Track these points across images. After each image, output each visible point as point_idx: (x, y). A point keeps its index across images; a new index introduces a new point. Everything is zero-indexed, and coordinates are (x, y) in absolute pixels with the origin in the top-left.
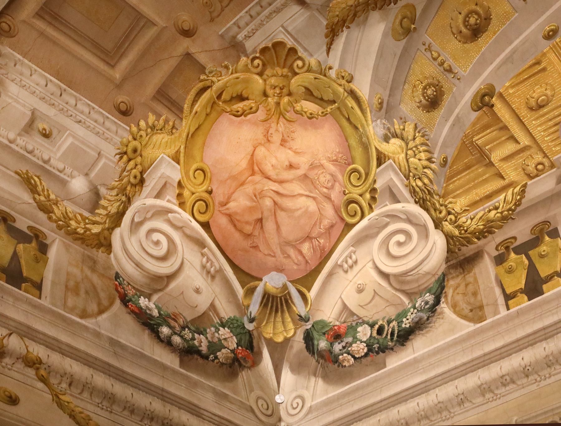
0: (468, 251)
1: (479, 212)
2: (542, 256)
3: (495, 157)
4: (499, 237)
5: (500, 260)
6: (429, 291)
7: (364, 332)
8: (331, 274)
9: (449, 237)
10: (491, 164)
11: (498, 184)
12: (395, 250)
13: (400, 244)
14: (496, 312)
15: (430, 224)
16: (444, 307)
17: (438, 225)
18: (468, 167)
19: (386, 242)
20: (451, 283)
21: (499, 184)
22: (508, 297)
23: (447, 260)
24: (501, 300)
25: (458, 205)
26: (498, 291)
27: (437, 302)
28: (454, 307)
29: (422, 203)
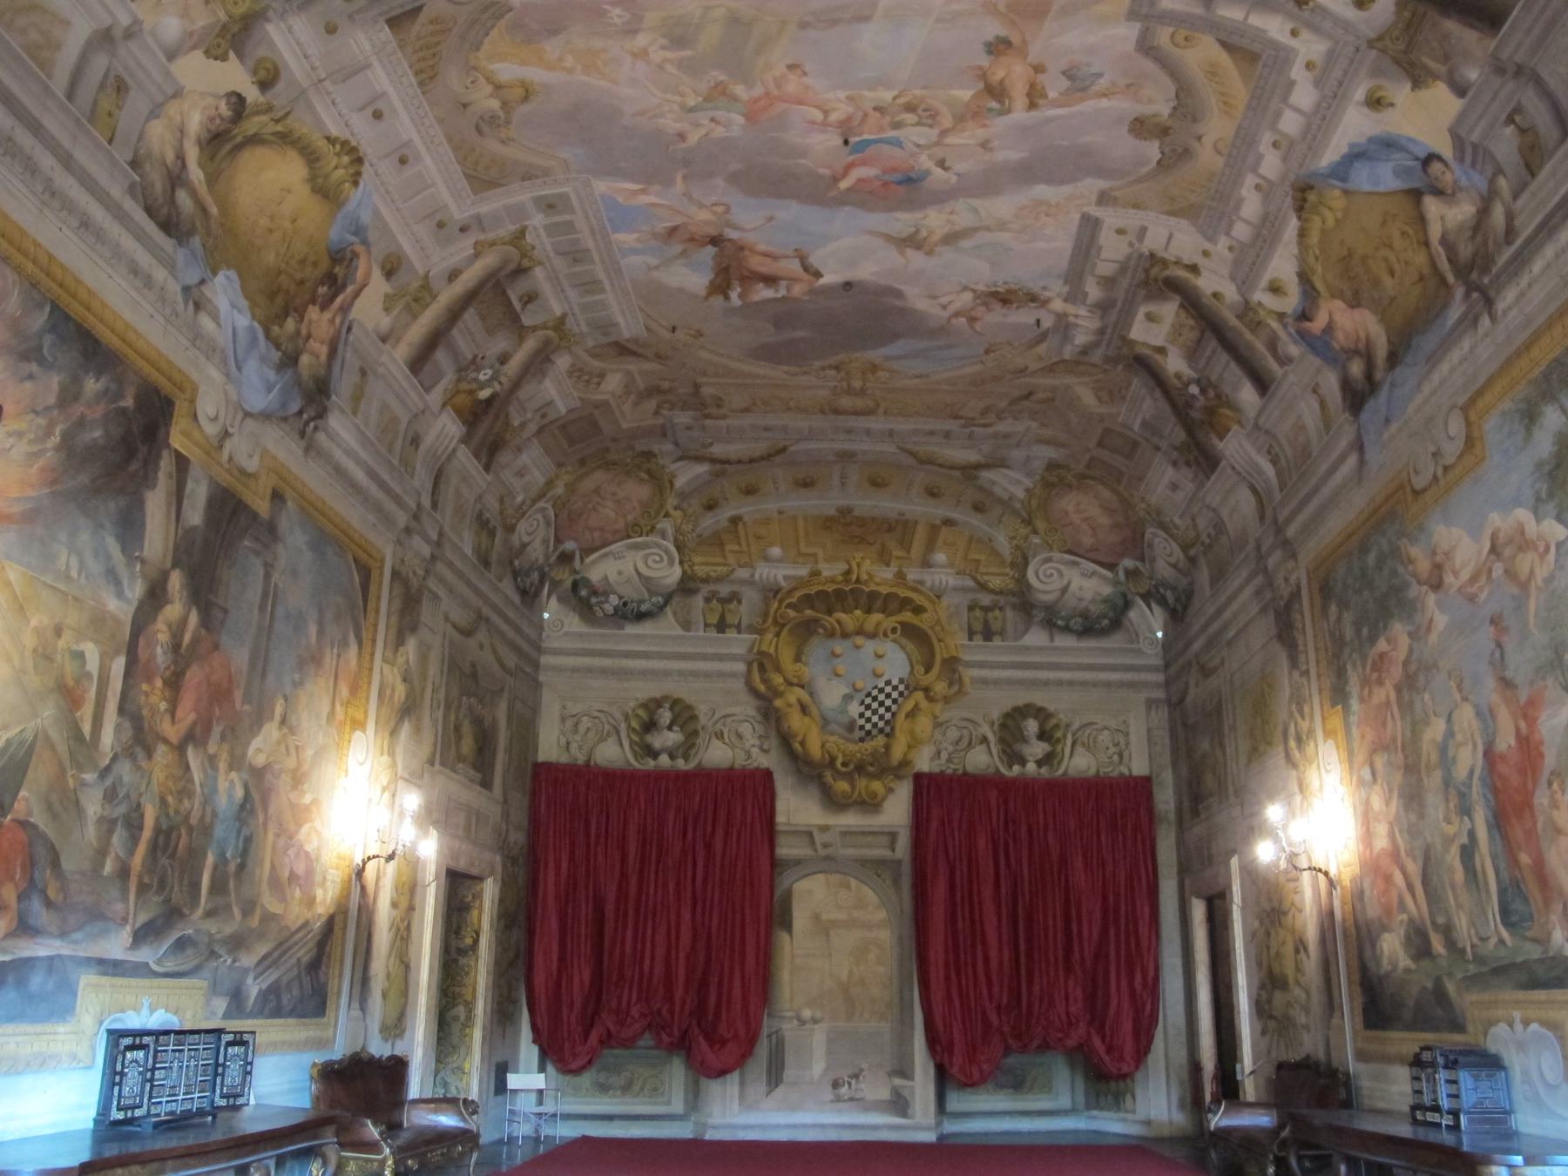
0: (691, 585)
1: (707, 569)
2: (730, 611)
3: (728, 548)
4: (711, 587)
5: (708, 600)
6: (662, 595)
7: (614, 600)
8: (605, 555)
9: (684, 572)
10: (723, 550)
11: (721, 560)
12: (650, 563)
13: (655, 561)
14: (697, 630)
15: (677, 561)
16: (668, 610)
17: (681, 563)
18: (711, 545)
19: (647, 557)
20: (676, 600)
21: (721, 560)
22: (706, 625)
23: (679, 584)
24: (702, 626)
25: (697, 559)
26: (701, 618)
27: (666, 603)
28: (675, 614)
29: (678, 548)
